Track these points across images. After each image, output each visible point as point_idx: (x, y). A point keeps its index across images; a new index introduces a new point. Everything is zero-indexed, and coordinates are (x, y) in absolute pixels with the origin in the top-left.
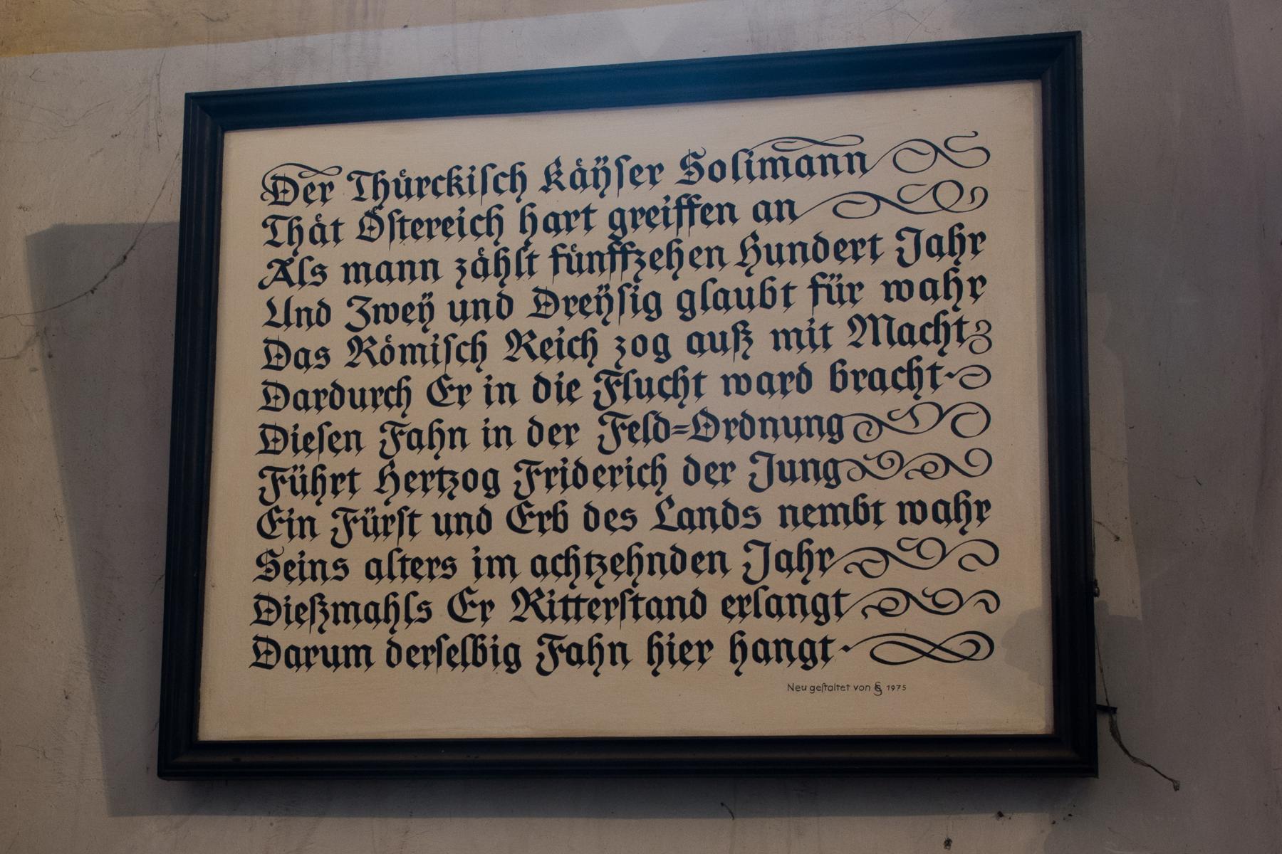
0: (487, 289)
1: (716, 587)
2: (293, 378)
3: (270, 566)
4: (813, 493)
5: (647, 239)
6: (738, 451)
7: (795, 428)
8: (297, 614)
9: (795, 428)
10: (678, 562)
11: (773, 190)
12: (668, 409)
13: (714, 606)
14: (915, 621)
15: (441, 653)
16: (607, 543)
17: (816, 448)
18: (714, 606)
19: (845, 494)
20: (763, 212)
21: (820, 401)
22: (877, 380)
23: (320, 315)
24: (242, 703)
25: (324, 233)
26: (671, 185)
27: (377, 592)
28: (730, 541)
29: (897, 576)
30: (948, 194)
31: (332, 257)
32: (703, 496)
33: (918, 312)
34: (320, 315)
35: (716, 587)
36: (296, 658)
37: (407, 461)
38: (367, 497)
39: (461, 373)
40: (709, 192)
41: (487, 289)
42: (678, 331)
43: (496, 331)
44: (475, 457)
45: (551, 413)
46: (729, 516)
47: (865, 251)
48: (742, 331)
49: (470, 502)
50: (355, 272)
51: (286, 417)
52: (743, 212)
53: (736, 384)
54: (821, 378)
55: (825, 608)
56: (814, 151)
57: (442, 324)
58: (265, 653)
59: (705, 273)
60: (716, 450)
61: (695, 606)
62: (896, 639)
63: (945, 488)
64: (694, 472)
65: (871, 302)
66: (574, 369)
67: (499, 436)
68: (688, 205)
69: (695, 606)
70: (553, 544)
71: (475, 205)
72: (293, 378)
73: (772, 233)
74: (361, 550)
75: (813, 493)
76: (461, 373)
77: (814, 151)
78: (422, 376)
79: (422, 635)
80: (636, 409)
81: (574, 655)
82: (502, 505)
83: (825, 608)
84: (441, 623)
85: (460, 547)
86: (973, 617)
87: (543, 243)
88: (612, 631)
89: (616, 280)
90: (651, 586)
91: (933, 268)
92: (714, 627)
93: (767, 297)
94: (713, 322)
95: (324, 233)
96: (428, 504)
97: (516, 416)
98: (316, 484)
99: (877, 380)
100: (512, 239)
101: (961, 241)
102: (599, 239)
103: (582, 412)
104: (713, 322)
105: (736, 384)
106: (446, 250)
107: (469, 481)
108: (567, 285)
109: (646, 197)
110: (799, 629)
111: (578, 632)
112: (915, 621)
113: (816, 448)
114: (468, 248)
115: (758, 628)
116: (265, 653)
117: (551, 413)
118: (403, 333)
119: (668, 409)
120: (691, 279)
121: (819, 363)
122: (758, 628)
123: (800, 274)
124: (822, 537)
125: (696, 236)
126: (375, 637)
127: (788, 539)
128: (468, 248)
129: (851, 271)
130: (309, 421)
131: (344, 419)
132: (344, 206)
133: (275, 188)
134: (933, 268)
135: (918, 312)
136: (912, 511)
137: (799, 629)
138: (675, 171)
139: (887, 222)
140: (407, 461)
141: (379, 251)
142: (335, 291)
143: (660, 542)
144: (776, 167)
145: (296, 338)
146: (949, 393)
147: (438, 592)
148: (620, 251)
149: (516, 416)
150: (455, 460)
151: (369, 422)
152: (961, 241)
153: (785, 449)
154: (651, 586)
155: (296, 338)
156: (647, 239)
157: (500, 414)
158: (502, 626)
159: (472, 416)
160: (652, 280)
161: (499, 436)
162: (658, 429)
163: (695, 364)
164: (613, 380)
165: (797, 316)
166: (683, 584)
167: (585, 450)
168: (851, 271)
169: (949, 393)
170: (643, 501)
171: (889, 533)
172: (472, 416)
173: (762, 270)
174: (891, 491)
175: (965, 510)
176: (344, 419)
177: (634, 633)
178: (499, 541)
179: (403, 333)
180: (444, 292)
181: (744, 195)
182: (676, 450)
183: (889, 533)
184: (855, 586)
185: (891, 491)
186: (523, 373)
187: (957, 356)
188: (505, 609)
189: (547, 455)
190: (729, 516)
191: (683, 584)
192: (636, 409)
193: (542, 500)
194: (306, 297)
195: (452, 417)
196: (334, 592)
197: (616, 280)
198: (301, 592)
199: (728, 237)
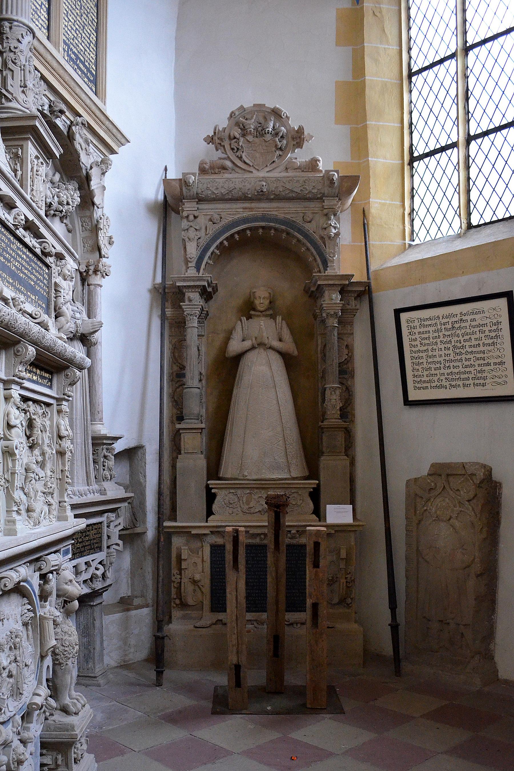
0: (436, 334)
1: (471, 376)
2: (413, 349)
3: (414, 376)
4: (482, 362)
5: (457, 325)
6: (471, 356)
7: (479, 352)
8: (418, 382)
9: (479, 352)
10: (465, 373)
11: (472, 317)
12: (462, 351)
13: (471, 379)
14: (497, 380)
15: (436, 387)
16: (456, 370)
17: (482, 355)
18: (471, 379)
19: (486, 362)
20: (471, 321)
21: (482, 348)
22: (489, 345)
23: (416, 340)
24: (413, 396)
25: (415, 328)
26: (459, 317)
27: (428, 379)
28: (472, 369)
29: (494, 373)
30: (496, 316)
31: (416, 331)
32: (467, 363)
33: (493, 334)
34: (416, 340)
35: (471, 376)
36: (419, 388)
37: (430, 360)
38: (425, 366)
39: (435, 347)
40: (464, 318)
41: (436, 334)
42: (462, 339)
43: (438, 340)
44: (438, 359)
45: (447, 352)
46: (472, 366)
47: (485, 325)
48: (470, 338)
49: (438, 365)
50: (419, 333)
51: (414, 355)
52: (469, 321)
53: (470, 346)
54: (481, 345)
55: (485, 378)
56: (477, 311)
57: (431, 340)
58: (415, 388)
59: (465, 330)
60: (468, 357)
61: (468, 379)
62: (494, 382)
63: (499, 360)
64: (466, 360)
65: (487, 333)
66: (449, 345)
67: (441, 356)
68: (461, 320)
69: (468, 379)
70: (449, 371)
71: (434, 322)
72: (413, 349)
73: (473, 323)
74: (425, 373)
75: (482, 362)
76: (435, 347)
77: (477, 311)
78: (430, 348)
79: (434, 384)
80: (458, 351)
81: (454, 386)
82: (442, 366)
83: (485, 378)
84: (436, 383)
85: (437, 372)
86: (504, 379)
87: (443, 327)
88: (458, 383)
89: (453, 332)
90: (462, 376)
91: (495, 327)
92: (471, 382)
93: (473, 333)
94: (467, 337)
95: (415, 328)
96: (433, 366)
97: (442, 353)
98: (418, 364)
99: (489, 345)
100: (439, 327)
101: (498, 323)
102: (450, 326)
103: (451, 352)
104: (467, 337)
105: (470, 346)
106: (431, 329)
107: (438, 362)
108: (447, 333)
109: (456, 319)
110: (482, 381)
111: (453, 383)
112: (497, 380)
113: (482, 355)
114: (433, 328)
115: (477, 381)
116: (415, 388)
117: (447, 352)
118: (427, 342)
119: (462, 351)
120: (463, 331)
121: (481, 343)
122: (477, 381)
123: (477, 329)
124: (484, 368)
125: (463, 325)
126: (428, 385)
127: (479, 369)
128: (433, 328)
129: (484, 329)
130: (416, 355)
131: (421, 354)
132: (417, 324)
133: (408, 321)
134: (495, 327)
135: (493, 334)
136: (495, 364)
137: (482, 381)
138: (459, 315)
139: (489, 320)
140: (430, 360)
141: (422, 330)
142: (417, 336)
143: (463, 370)
144: (473, 313)
145: (413, 343)
146: (498, 346)
147: (436, 378)
148: (453, 327)
149: (442, 353)
150: (435, 359)
151: (424, 355)
152: (498, 323)
153: (478, 356)
154: (462, 376)
155: (413, 343)
156: (457, 325)
157: (440, 353)
158: (444, 383)
159: (436, 353)
160: (458, 332)
161: (441, 356)
162: (461, 354)
163: (465, 344)
164: (454, 347)
165: (477, 336)
166: (466, 376)
167: (452, 357)
168: (484, 329)
169: (498, 346)
170: (460, 364)
171: (492, 367)
172: (436, 353)
173: (472, 329)
174: (492, 361)
175: (502, 363)
176: (421, 354)
177: (461, 383)
178: (442, 371)
179: (427, 342)
180: (431, 335)
181: (469, 318)
182: (464, 356)
183: (492, 367)
184: (488, 375)
185: (492, 361)
186: (443, 346)
187: (499, 341)
188: (444, 380)
189: (447, 358)
190: (472, 366)
191: (466, 376)
192: (458, 351)
193: (447, 365)
194: (413, 337)
195: (434, 353)
196: (423, 379)
197: (453, 332)
198: (419, 379)
199: (467, 324)
